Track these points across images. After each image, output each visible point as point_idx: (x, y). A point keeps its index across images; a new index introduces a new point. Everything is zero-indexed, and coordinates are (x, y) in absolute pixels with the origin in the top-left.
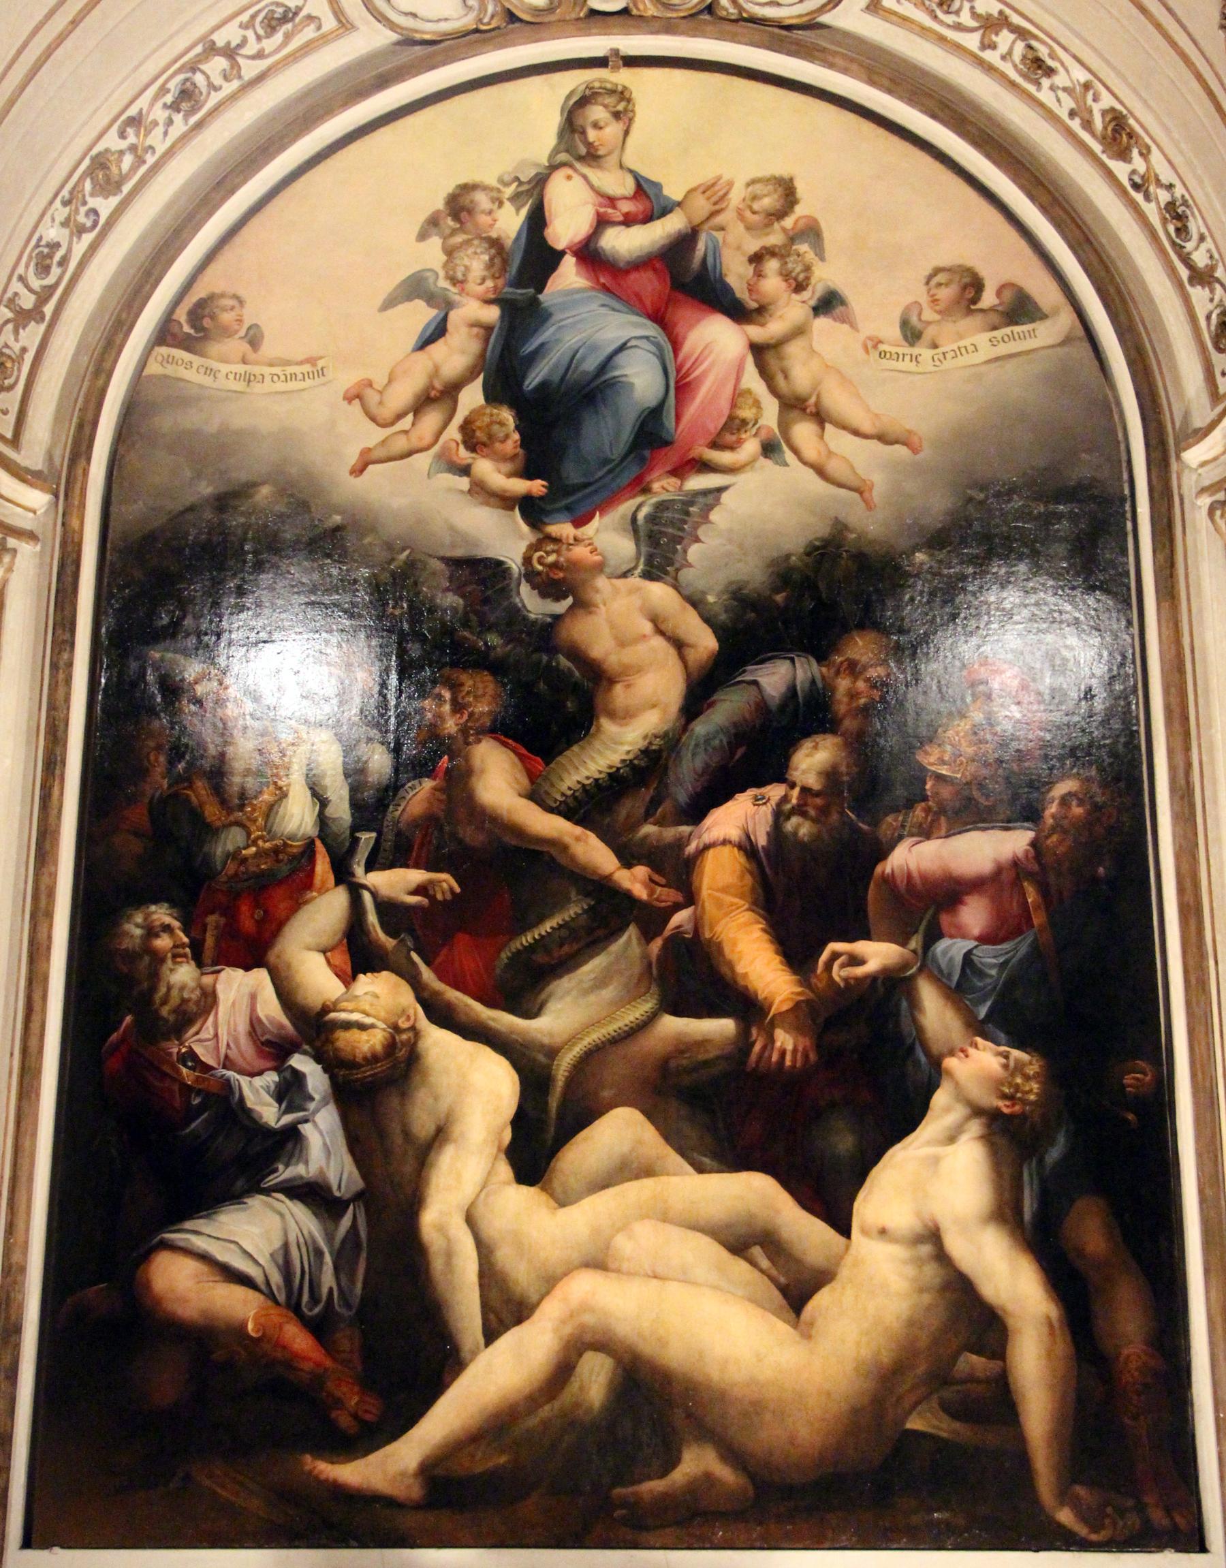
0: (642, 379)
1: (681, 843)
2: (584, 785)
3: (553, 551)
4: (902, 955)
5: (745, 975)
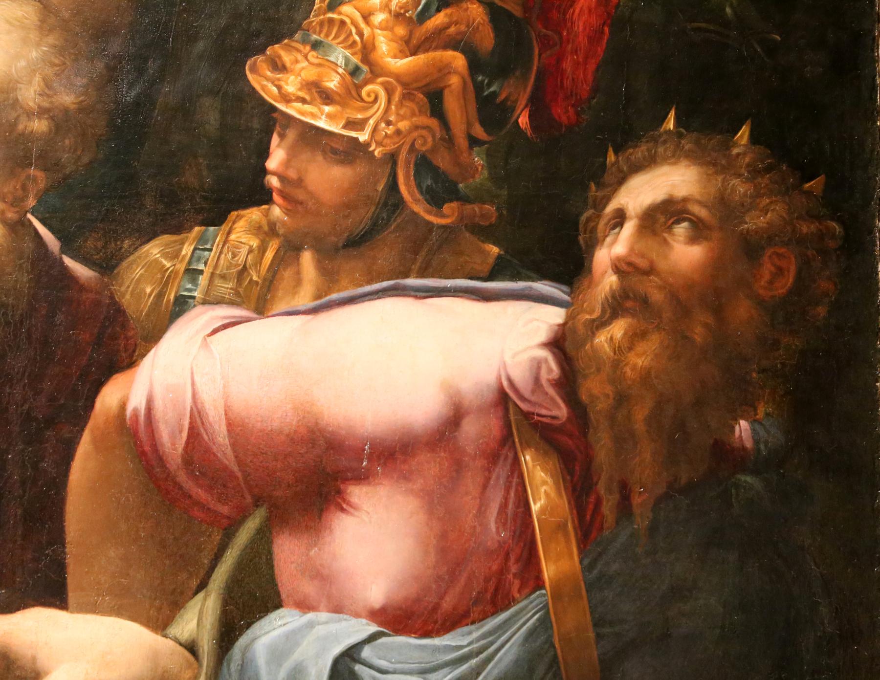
4: (155, 656)
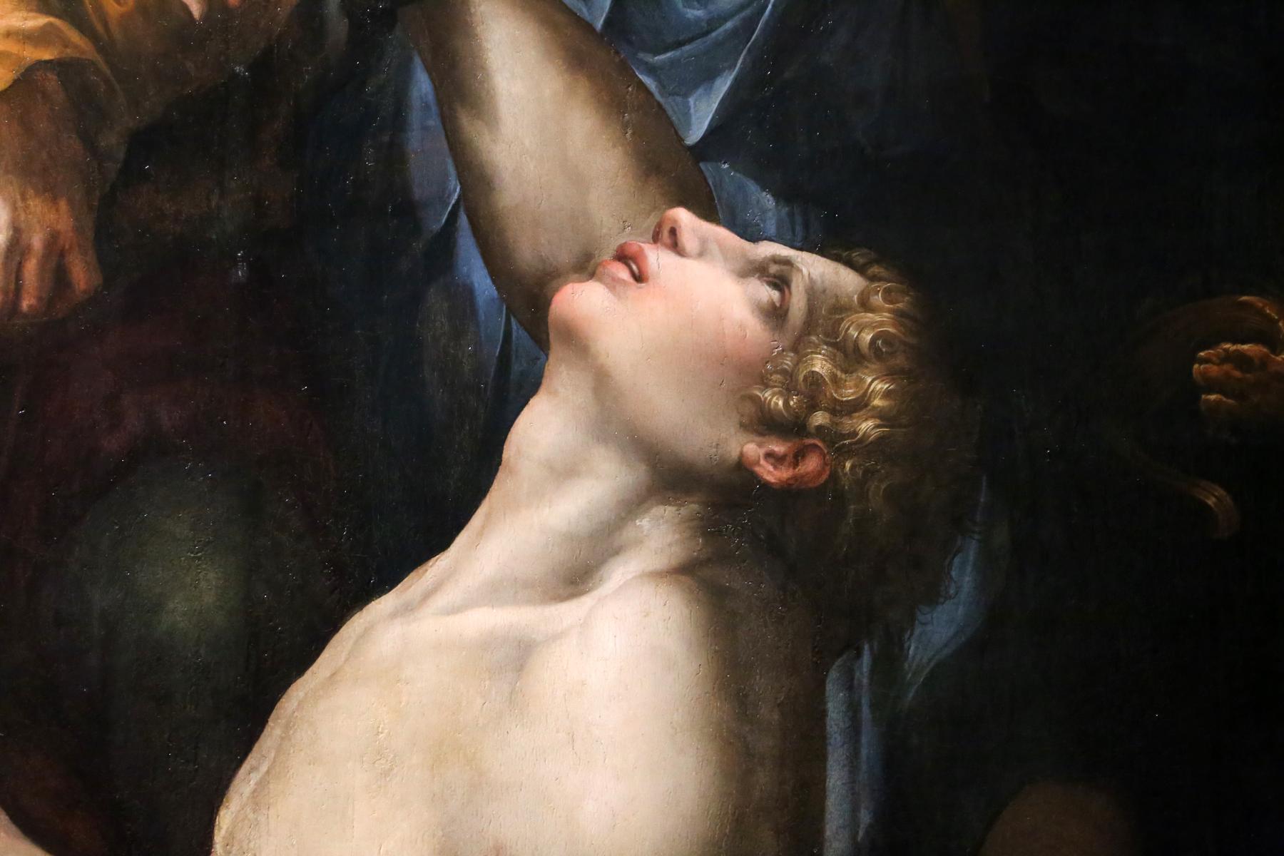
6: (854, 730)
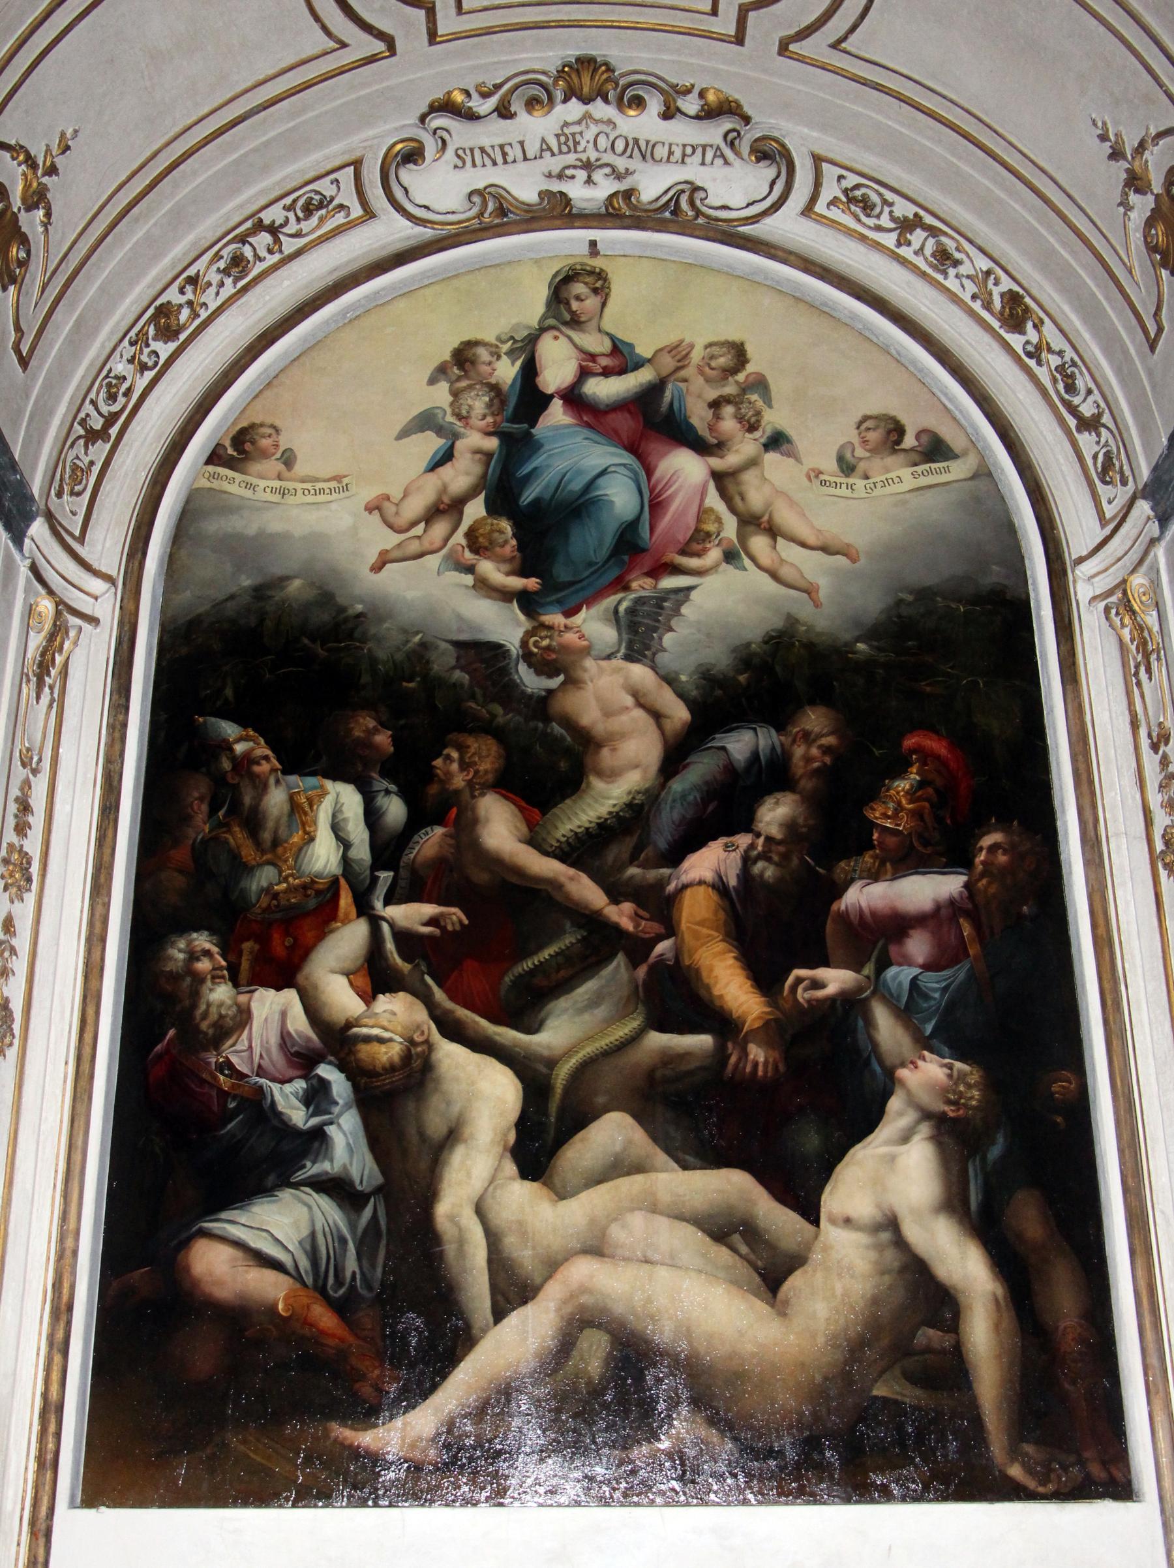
0: (621, 498)
1: (661, 884)
2: (576, 833)
3: (546, 637)
4: (857, 980)
5: (721, 997)
6: (976, 1176)
